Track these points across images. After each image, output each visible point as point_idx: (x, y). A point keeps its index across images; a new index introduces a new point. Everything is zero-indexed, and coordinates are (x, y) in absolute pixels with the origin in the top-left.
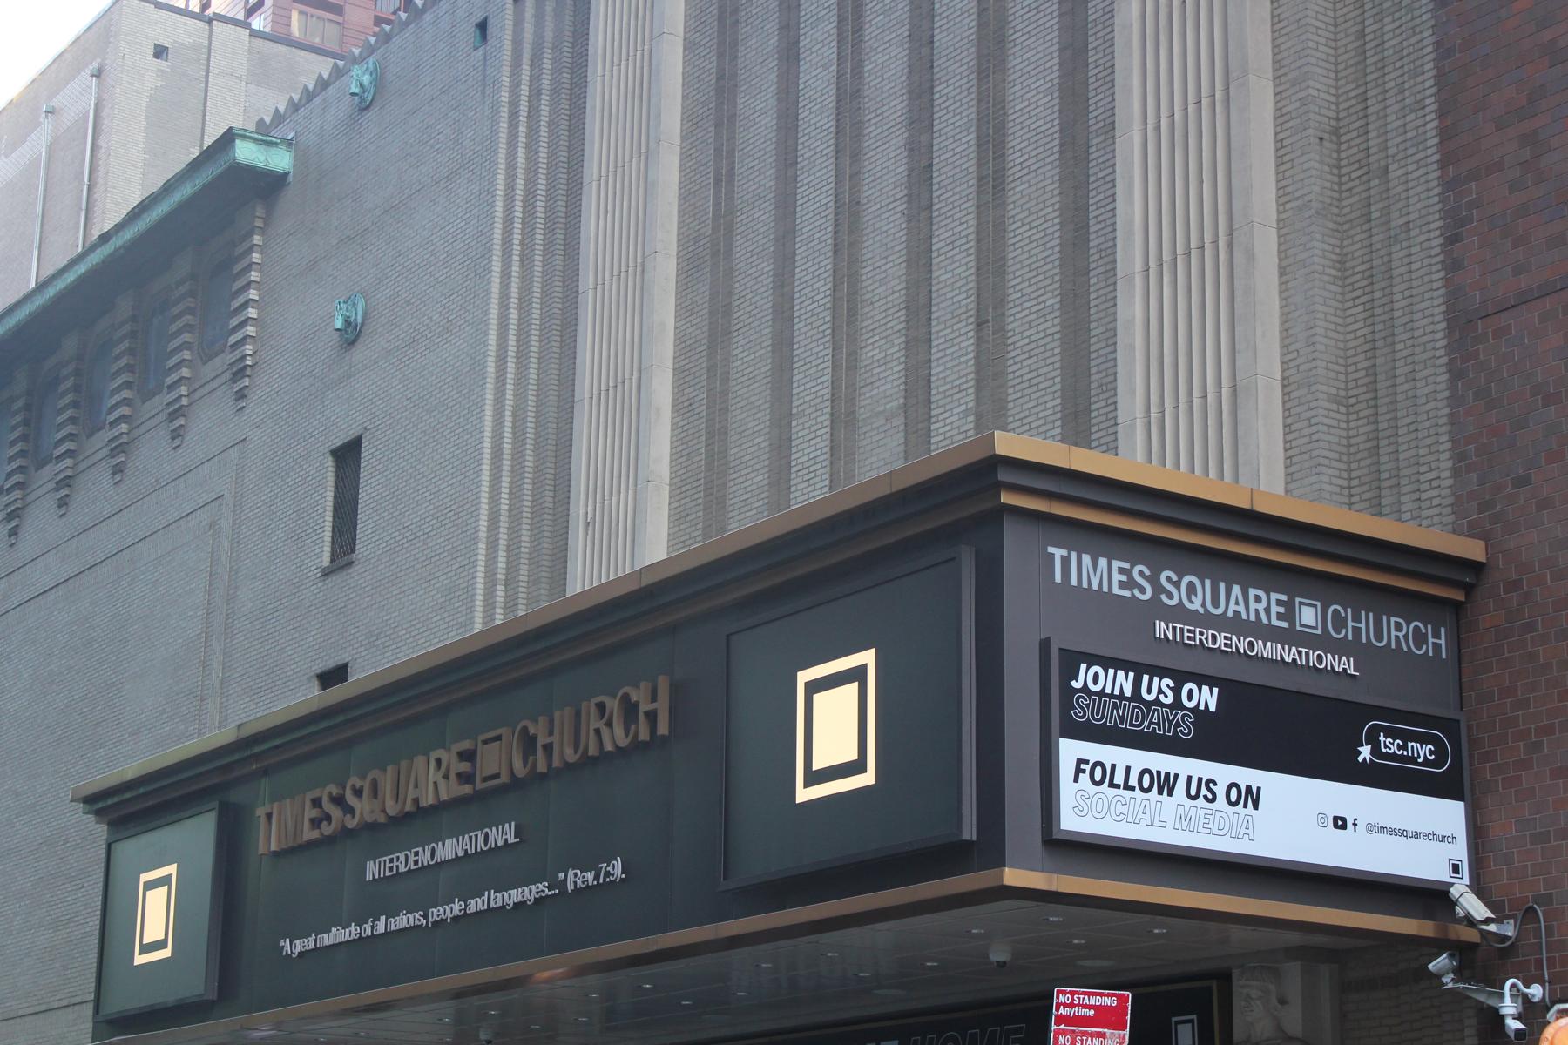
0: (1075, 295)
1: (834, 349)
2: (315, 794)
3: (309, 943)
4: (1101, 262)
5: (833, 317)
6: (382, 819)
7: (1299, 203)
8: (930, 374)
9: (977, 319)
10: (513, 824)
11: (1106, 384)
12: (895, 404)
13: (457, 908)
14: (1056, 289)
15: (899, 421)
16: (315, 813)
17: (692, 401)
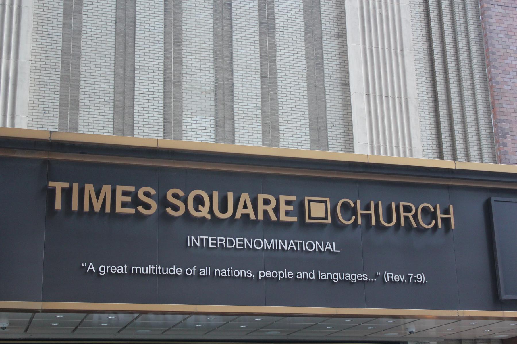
0: (316, 86)
1: (164, 51)
2: (132, 189)
3: (123, 269)
4: (330, 80)
5: (165, 38)
6: (208, 217)
7: (422, 98)
8: (233, 84)
9: (261, 74)
10: (334, 243)
11: (336, 124)
12: (208, 88)
13: (290, 274)
14: (305, 80)
15: (212, 96)
16: (128, 199)
17: (51, 33)
